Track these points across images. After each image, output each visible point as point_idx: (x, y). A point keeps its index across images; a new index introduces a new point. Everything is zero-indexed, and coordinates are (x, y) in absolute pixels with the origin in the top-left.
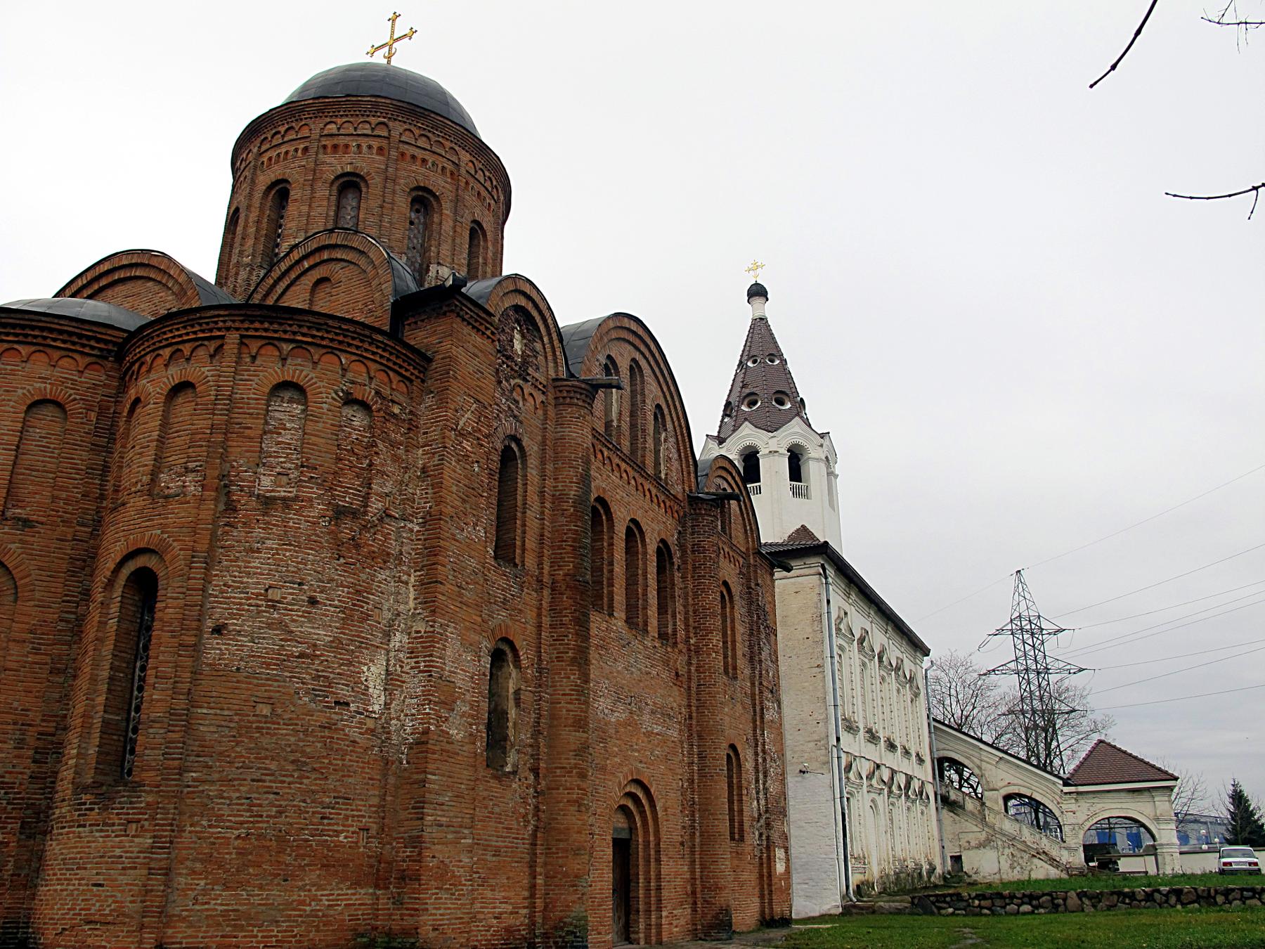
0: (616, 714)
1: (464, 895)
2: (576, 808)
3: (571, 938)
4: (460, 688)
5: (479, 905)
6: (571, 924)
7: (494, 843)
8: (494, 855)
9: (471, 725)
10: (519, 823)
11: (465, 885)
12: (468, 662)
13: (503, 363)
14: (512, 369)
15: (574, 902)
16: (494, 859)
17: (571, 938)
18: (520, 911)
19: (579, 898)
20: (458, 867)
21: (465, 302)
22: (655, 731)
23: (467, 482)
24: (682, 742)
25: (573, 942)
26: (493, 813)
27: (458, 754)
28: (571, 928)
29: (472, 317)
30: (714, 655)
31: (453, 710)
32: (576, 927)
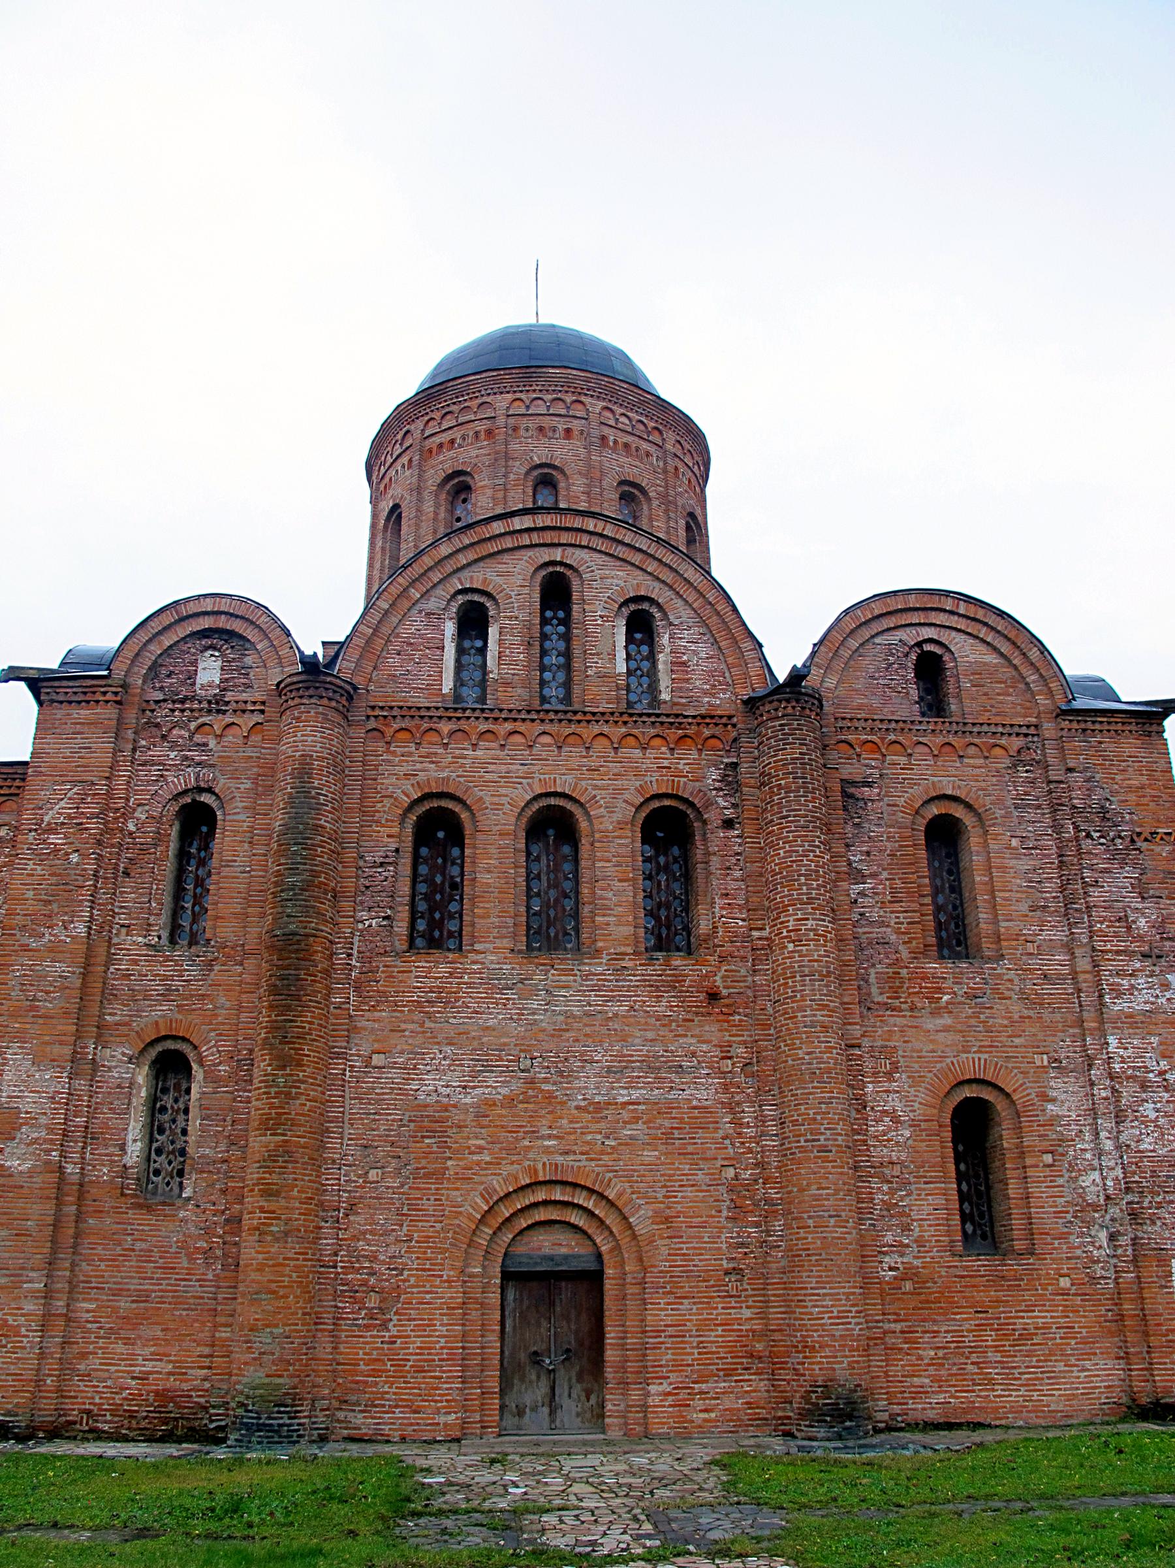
0: (479, 1091)
1: (24, 1348)
2: (256, 1238)
3: (241, 1411)
4: (27, 1113)
5: (98, 1361)
6: (242, 1393)
7: (132, 1287)
8: (133, 1301)
9: (48, 1152)
10: (191, 1260)
11: (27, 1336)
12: (46, 1080)
13: (173, 711)
14: (192, 710)
15: (246, 1364)
16: (135, 1305)
17: (241, 1411)
18: (190, 1371)
19: (255, 1359)
20: (16, 1315)
21: (56, 684)
22: (621, 1100)
23: (54, 880)
24: (731, 1107)
25: (243, 1417)
26: (133, 1250)
27: (22, 1187)
28: (241, 1399)
29: (75, 693)
30: (791, 947)
31: (14, 1138)
32: (248, 1397)
